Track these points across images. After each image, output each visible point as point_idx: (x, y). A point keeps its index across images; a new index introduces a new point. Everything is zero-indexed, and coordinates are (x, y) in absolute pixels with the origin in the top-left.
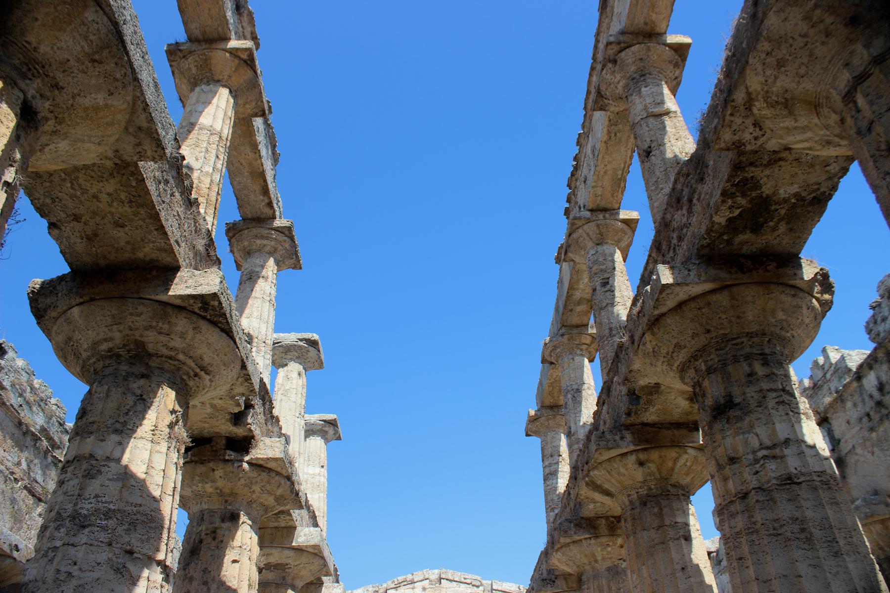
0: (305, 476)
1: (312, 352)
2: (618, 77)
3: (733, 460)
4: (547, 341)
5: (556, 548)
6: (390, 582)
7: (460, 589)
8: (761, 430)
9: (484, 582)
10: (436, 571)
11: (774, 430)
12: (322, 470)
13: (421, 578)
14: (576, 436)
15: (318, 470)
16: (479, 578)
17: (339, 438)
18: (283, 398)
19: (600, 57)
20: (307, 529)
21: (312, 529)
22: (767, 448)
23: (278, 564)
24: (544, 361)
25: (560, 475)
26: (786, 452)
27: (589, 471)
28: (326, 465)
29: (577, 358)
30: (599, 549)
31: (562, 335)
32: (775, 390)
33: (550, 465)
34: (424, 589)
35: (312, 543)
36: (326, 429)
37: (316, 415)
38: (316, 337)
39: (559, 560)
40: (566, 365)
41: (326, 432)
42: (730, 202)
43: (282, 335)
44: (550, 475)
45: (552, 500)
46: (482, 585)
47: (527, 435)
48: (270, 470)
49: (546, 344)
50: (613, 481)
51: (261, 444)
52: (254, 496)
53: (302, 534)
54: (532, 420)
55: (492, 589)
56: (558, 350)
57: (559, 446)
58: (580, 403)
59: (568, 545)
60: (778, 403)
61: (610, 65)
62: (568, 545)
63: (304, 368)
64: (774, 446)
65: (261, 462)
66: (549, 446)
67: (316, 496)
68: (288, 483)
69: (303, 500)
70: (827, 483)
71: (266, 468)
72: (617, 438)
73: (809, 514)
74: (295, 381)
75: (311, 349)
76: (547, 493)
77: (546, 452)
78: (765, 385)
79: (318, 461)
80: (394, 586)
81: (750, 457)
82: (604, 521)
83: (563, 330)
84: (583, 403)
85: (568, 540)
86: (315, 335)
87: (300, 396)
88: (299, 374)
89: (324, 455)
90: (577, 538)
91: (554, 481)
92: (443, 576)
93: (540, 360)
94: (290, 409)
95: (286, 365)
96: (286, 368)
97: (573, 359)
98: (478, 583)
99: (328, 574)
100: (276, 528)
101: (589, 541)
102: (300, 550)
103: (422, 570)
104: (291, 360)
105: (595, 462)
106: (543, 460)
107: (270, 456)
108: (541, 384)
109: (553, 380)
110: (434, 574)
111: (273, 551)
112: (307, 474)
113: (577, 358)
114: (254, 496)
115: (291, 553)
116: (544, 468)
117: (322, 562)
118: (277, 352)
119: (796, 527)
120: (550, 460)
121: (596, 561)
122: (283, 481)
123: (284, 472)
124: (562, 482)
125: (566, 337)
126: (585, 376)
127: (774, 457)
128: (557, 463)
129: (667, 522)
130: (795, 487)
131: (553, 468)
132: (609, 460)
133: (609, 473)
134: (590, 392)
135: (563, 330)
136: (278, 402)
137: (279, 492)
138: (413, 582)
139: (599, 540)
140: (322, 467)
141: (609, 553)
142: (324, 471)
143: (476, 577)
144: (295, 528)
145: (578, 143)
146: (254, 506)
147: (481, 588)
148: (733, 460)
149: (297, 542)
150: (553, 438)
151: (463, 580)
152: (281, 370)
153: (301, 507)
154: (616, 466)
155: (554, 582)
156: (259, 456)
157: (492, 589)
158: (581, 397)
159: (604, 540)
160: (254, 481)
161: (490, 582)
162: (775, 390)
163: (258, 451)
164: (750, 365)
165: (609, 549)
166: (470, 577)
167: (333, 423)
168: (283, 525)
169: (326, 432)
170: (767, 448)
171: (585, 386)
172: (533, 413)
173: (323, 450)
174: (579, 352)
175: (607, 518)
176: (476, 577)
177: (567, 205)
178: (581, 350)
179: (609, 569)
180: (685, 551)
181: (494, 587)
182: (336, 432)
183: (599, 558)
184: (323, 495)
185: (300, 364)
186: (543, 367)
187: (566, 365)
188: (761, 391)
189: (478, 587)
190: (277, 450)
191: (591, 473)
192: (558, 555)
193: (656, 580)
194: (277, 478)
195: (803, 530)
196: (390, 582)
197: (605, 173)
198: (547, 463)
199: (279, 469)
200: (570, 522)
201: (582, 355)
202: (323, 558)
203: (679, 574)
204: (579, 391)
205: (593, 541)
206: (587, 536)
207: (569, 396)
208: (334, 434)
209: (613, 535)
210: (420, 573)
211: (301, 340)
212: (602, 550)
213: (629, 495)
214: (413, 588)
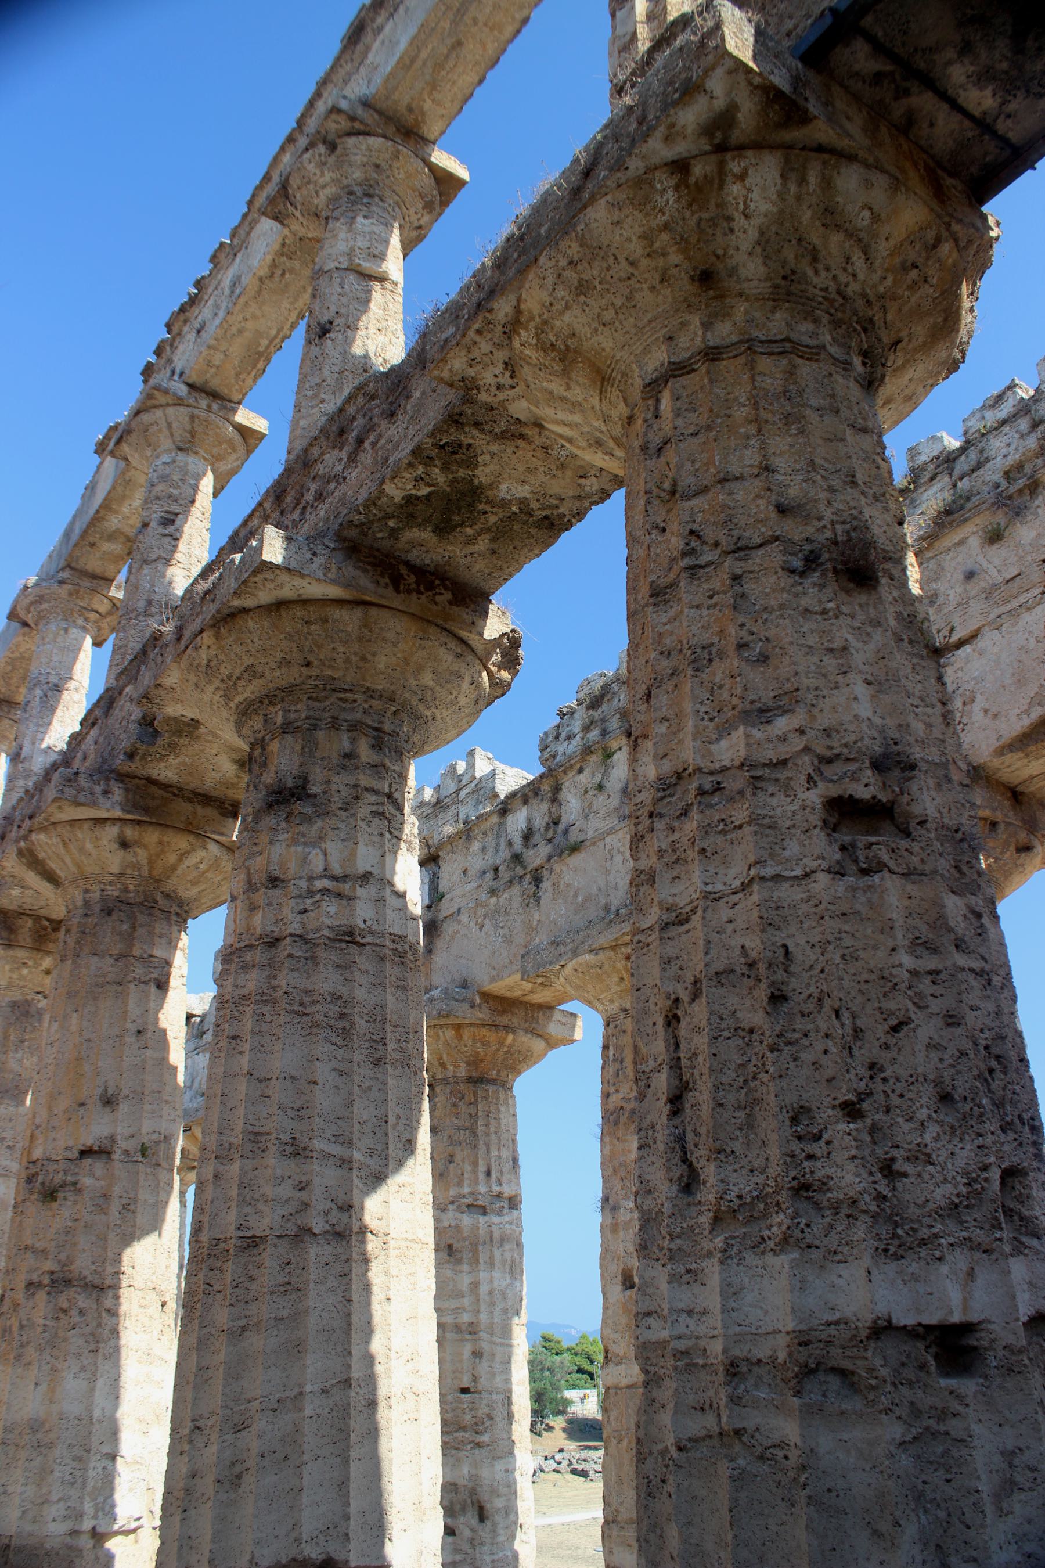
2: (328, 176)
3: (274, 882)
4: (30, 583)
8: (335, 849)
11: (353, 854)
14: (26, 765)
19: (312, 125)
22: (334, 878)
24: (12, 616)
26: (360, 892)
27: (31, 831)
29: (74, 632)
30: (7, 967)
31: (61, 582)
32: (376, 792)
40: (51, 636)
42: (420, 470)
49: (26, 587)
50: (68, 860)
56: (45, 606)
58: (53, 710)
60: (375, 814)
61: (322, 149)
64: (345, 878)
70: (401, 955)
72: (98, 789)
73: (360, 994)
78: (365, 781)
81: (303, 884)
82: (30, 923)
83: (65, 575)
84: (59, 712)
93: (6, 610)
97: (66, 630)
105: (46, 819)
109: (17, 655)
113: (74, 632)
119: (334, 1010)
127: (339, 895)
129: (137, 952)
130: (354, 949)
132: (72, 823)
133: (65, 844)
134: (76, 697)
135: (65, 575)
139: (11, 953)
141: (22, 978)
145: (214, 259)
148: (274, 882)
154: (80, 836)
159: (21, 954)
162: (376, 792)
164: (353, 741)
165: (25, 971)
170: (334, 878)
171: (71, 685)
174: (80, 621)
175: (37, 918)
177: (153, 359)
178: (86, 620)
180: (152, 1005)
186: (8, 626)
187: (51, 636)
188: (355, 786)
191: (34, 836)
193: (89, 1040)
195: (342, 1016)
197: (240, 331)
201: (84, 629)
203: (130, 1039)
204: (58, 689)
207: (38, 692)
209: (39, 950)
212: (11, 970)
213: (87, 891)
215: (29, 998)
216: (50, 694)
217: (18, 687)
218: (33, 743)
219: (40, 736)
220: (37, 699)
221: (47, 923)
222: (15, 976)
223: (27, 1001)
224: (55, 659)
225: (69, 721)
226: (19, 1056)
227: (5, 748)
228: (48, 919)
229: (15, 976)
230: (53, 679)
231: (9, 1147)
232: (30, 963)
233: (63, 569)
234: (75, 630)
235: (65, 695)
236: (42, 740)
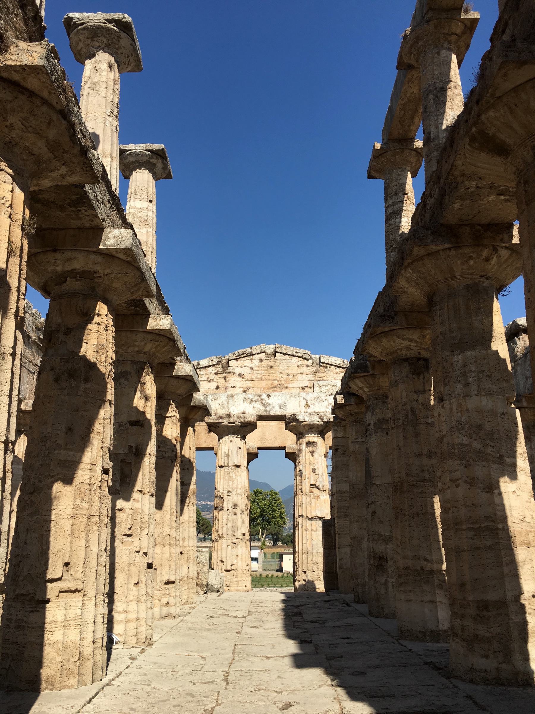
0: (132, 211)
1: (125, 41)
4: (408, 32)
5: (406, 264)
6: (231, 354)
7: (293, 361)
9: (313, 356)
10: (272, 346)
12: (151, 204)
13: (258, 351)
14: (436, 142)
15: (146, 204)
16: (309, 353)
17: (169, 176)
18: (91, 92)
20: (116, 232)
21: (123, 230)
23: (84, 272)
25: (404, 214)
27: (479, 115)
28: (154, 200)
29: (444, 52)
30: (459, 262)
31: (428, 22)
33: (394, 204)
34: (261, 360)
35: (123, 246)
36: (154, 161)
37: (142, 145)
38: (128, 18)
39: (408, 280)
41: (154, 165)
43: (86, 14)
44: (393, 213)
45: (394, 239)
46: (311, 358)
47: (370, 177)
48: (31, 94)
49: (406, 36)
51: (12, 49)
52: (14, 134)
53: (111, 236)
54: (377, 155)
55: (320, 362)
56: (421, 43)
57: (405, 184)
59: (421, 258)
62: (421, 258)
63: (115, 61)
65: (16, 77)
66: (394, 184)
67: (144, 230)
68: (64, 122)
69: (97, 168)
71: (26, 89)
74: (104, 73)
75: (123, 34)
76: (388, 234)
77: (390, 190)
79: (145, 195)
80: (234, 357)
82: (468, 230)
83: (430, 15)
84: (448, 104)
85: (423, 252)
86: (126, 15)
87: (111, 91)
88: (110, 66)
89: (152, 189)
90: (433, 248)
91: (398, 220)
92: (277, 350)
93: (395, 64)
94: (99, 105)
95: (94, 55)
96: (93, 60)
97: (438, 53)
98: (307, 357)
99: (149, 295)
100: (79, 228)
101: (448, 252)
102: (110, 255)
103: (259, 344)
104: (99, 48)
106: (386, 200)
107: (26, 63)
108: (391, 110)
110: (270, 348)
111: (77, 255)
112: (134, 208)
113: (444, 52)
114: (14, 134)
115: (99, 259)
116: (386, 208)
117: (138, 274)
118: (81, 37)
120: (394, 199)
121: (453, 278)
122: (55, 117)
123: (54, 100)
124: (406, 224)
125: (432, 23)
126: (452, 73)
128: (402, 202)
131: (396, 207)
132: (515, 89)
134: (456, 91)
136: (85, 96)
137: (52, 134)
138: (251, 355)
140: (151, 201)
142: (153, 207)
143: (307, 352)
144: (103, 229)
146: (17, 150)
147: (311, 361)
149: (105, 245)
150: (399, 175)
151: (295, 354)
152: (87, 62)
153: (94, 180)
155: (393, 318)
156: (9, 63)
157: (320, 362)
158: (445, 97)
159: (467, 250)
160: (9, 106)
161: (318, 356)
163: (8, 56)
165: (472, 262)
166: (301, 351)
167: (159, 154)
168: (87, 225)
169: (154, 165)
171: (452, 85)
172: (378, 146)
173: (151, 185)
176: (307, 352)
179: (468, 287)
181: (322, 360)
182: (165, 167)
183: (457, 274)
184: (152, 231)
185: (111, 54)
186: (399, 73)
189: (308, 360)
190: (35, 54)
191: (483, 117)
192: (408, 273)
194: (44, 109)
196: (231, 354)
198: (390, 202)
199: (45, 94)
200: (427, 229)
201: (450, 49)
202: (139, 269)
205: (453, 252)
206: (447, 246)
207: (431, 97)
208: (163, 168)
210: (258, 347)
211: (110, 21)
212: (462, 264)
214: (251, 360)
215: (477, 281)
216: (439, 95)
217: (409, 126)
218: (437, 127)
219: (440, 121)
220: (432, 101)
221: (479, 227)
222: (465, 267)
223: (475, 283)
224: (436, 73)
225: (456, 107)
226: (479, 318)
227: (409, 168)
228: (479, 225)
229: (465, 267)
230: (438, 85)
231: (488, 376)
232: (474, 256)
233: (427, 13)
234: (444, 51)
235: (449, 92)
236: (442, 123)
